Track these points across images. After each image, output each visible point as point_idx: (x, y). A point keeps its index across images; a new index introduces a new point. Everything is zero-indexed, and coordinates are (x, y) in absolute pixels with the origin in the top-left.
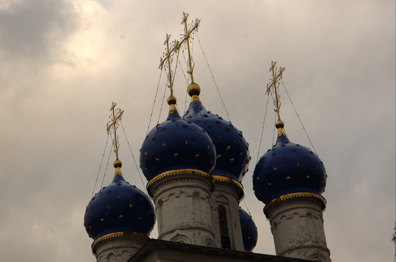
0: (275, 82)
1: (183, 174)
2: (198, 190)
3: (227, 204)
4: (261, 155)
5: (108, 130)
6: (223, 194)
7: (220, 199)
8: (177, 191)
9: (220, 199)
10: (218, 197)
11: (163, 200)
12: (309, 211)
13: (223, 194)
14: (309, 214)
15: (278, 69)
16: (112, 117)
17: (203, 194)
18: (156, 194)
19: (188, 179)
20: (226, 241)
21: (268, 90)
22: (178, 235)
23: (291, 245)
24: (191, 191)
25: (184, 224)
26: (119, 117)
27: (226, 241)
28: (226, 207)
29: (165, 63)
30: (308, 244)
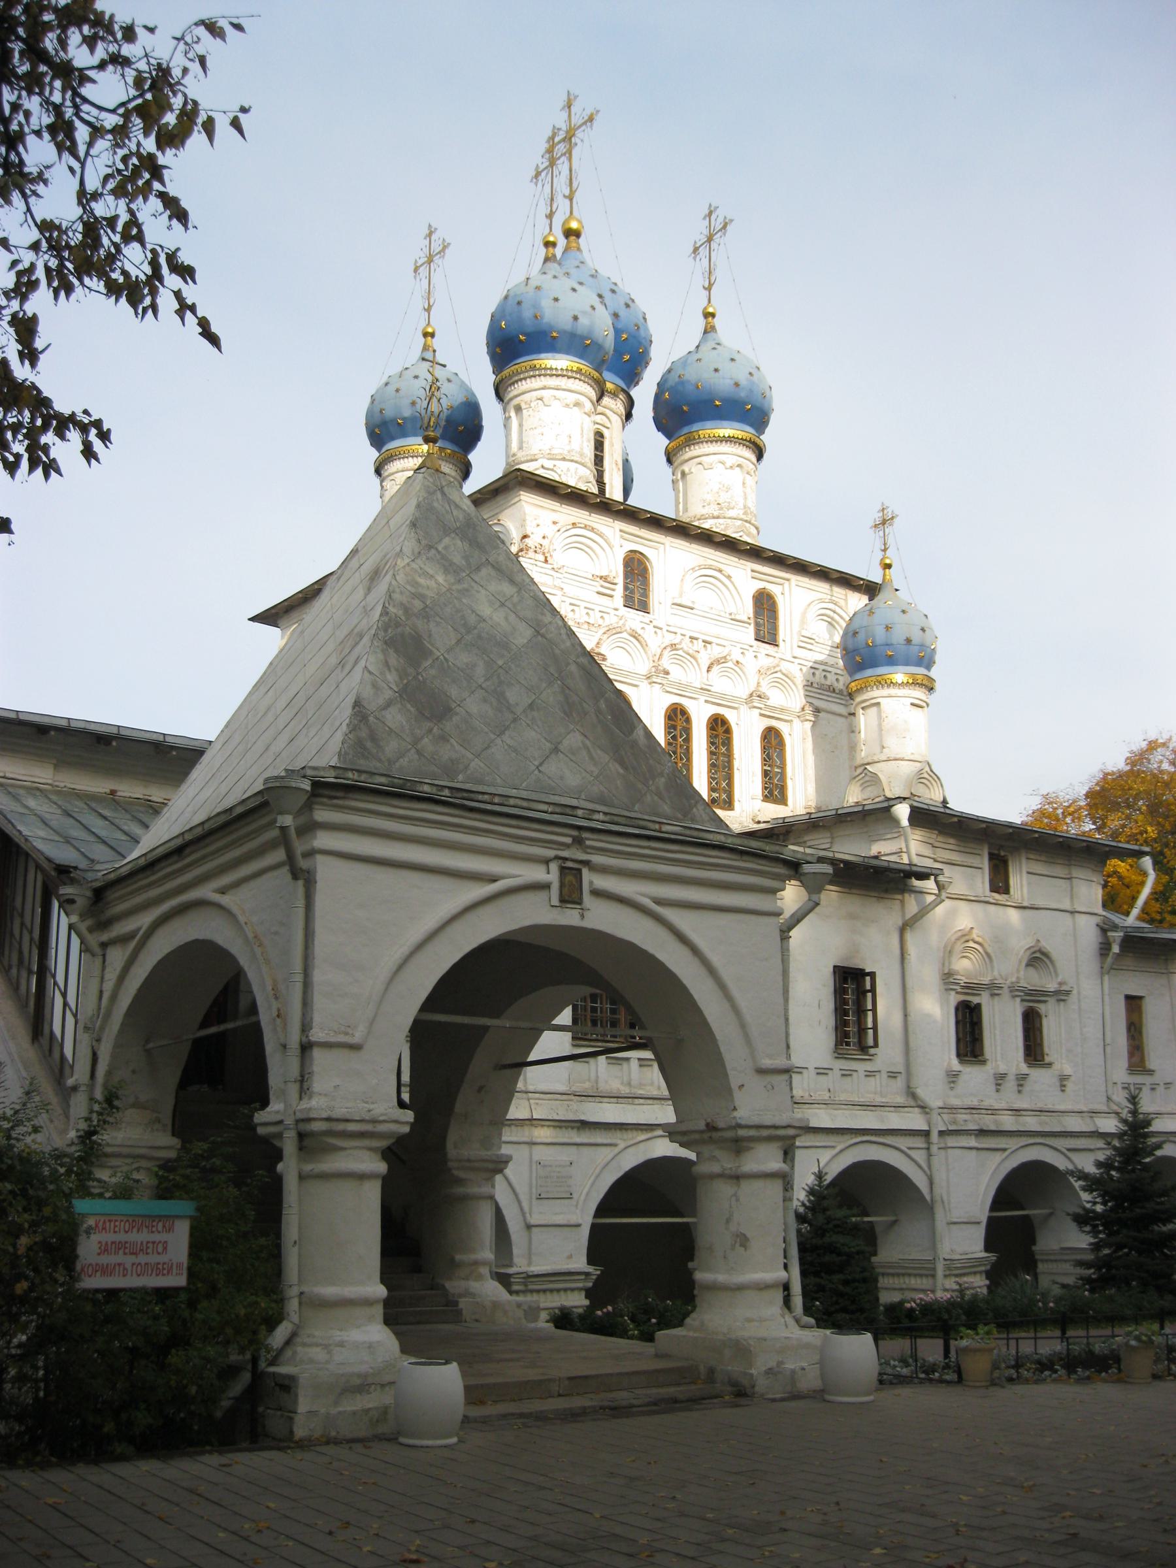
0: (710, 239)
4: (675, 357)
5: (416, 270)
8: (545, 393)
11: (523, 406)
15: (721, 219)
16: (426, 251)
18: (511, 395)
21: (696, 250)
23: (704, 511)
25: (554, 452)
26: (439, 253)
28: (606, 432)
29: (543, 174)
30: (731, 513)
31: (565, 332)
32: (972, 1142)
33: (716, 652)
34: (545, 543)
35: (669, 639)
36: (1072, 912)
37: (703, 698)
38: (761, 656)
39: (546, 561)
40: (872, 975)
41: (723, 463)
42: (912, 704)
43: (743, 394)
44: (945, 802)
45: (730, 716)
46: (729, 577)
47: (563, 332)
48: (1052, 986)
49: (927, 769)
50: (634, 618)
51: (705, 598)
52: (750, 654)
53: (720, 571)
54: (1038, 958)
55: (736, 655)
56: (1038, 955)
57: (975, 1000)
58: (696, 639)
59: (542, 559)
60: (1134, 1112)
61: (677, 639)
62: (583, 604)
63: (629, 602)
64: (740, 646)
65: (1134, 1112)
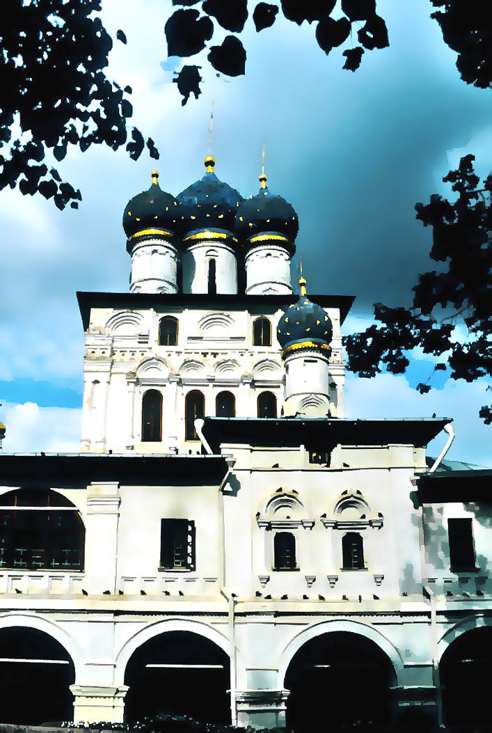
10: (208, 251)
22: (137, 287)
32: (271, 619)
33: (220, 358)
36: (389, 469)
38: (255, 354)
39: (100, 334)
40: (192, 523)
42: (306, 361)
44: (329, 415)
46: (228, 316)
52: (247, 354)
54: (347, 502)
55: (236, 356)
58: (207, 353)
61: (190, 357)
62: (128, 350)
64: (237, 351)
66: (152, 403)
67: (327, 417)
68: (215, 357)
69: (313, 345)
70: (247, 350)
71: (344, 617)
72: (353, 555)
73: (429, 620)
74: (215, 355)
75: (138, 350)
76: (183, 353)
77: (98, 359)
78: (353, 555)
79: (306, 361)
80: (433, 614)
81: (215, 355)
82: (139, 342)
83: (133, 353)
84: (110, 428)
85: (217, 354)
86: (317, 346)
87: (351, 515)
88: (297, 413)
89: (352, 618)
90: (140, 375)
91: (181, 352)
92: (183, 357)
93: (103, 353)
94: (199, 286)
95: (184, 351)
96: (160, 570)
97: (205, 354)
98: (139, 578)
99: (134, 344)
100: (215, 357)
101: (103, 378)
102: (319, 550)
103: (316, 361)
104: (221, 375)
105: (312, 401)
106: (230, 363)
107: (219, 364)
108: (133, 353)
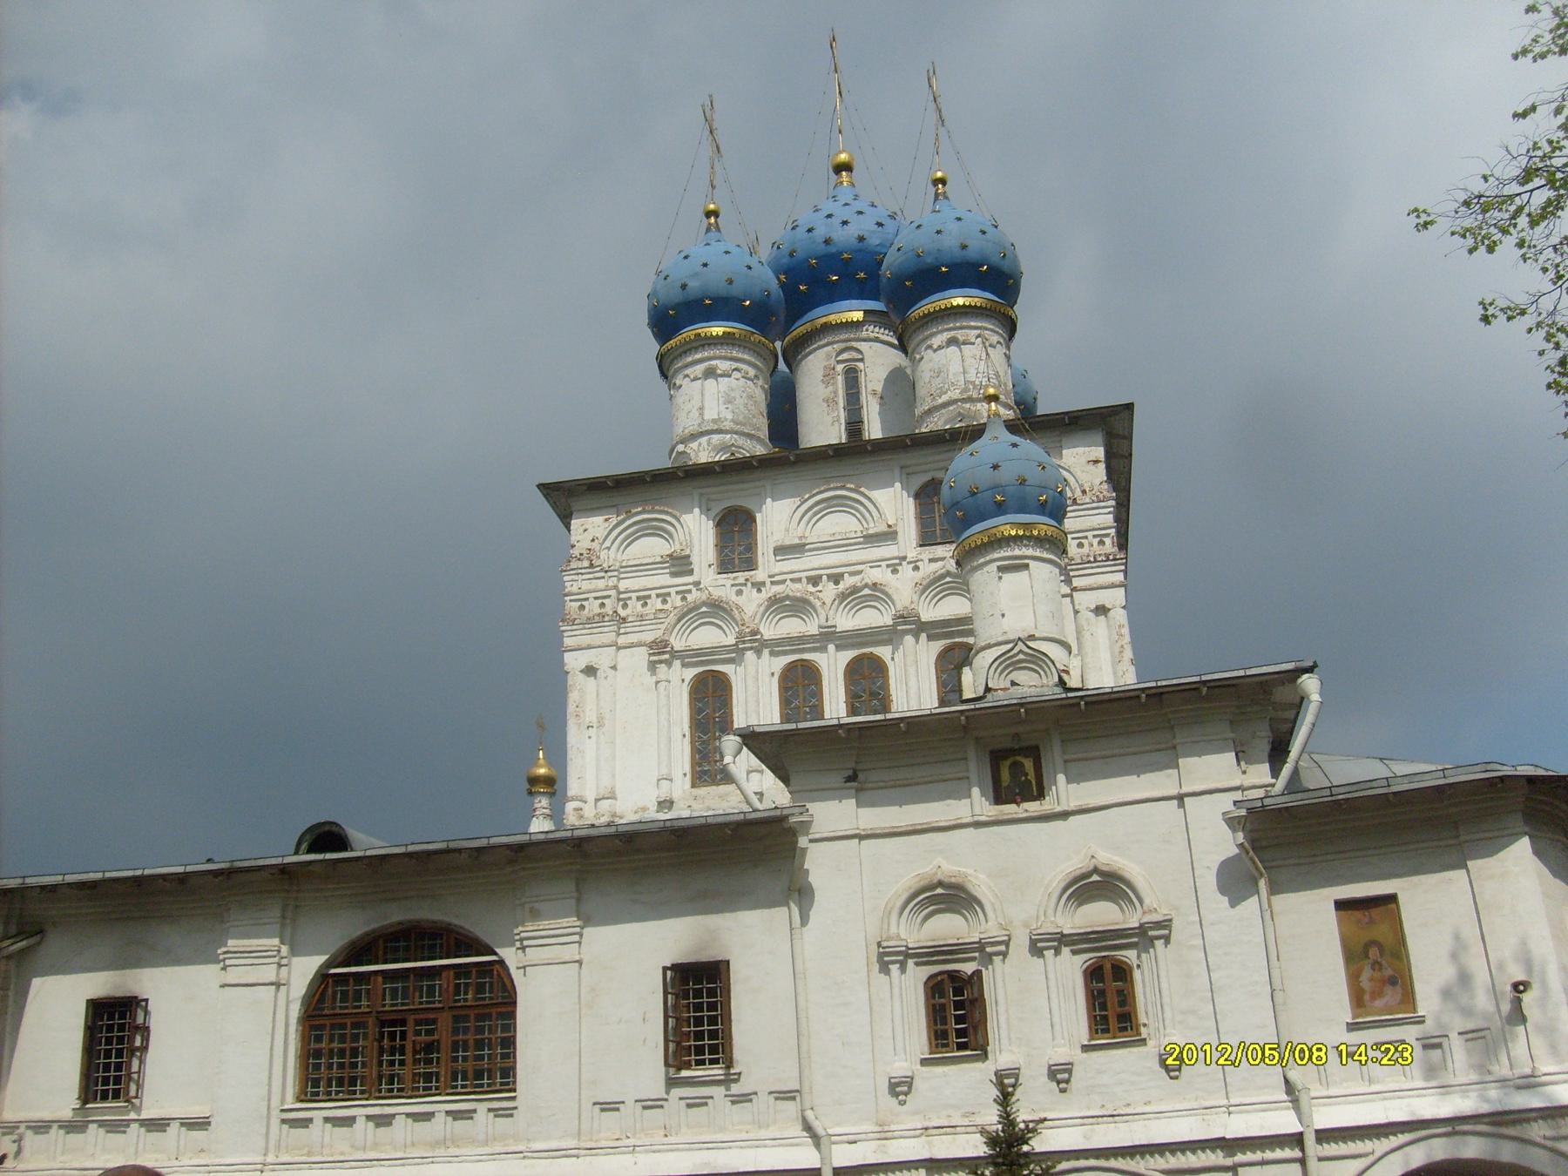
1: (682, 345)
2: (713, 362)
3: (862, 360)
6: (854, 344)
7: (845, 356)
9: (845, 356)
10: (839, 354)
12: (952, 333)
13: (854, 344)
14: (953, 341)
17: (723, 366)
19: (696, 348)
20: (855, 426)
24: (699, 369)
27: (855, 426)
30: (945, 398)
31: (678, 304)
33: (849, 581)
34: (595, 545)
35: (771, 591)
37: (831, 647)
39: (592, 566)
41: (930, 347)
42: (1001, 569)
43: (929, 260)
44: (1062, 682)
45: (883, 652)
47: (676, 307)
48: (1133, 922)
49: (1021, 646)
50: (720, 586)
51: (840, 524)
52: (906, 569)
53: (843, 488)
55: (879, 575)
56: (1095, 878)
57: (968, 968)
58: (820, 577)
59: (586, 563)
60: (1007, 1119)
62: (653, 593)
63: (725, 565)
64: (884, 564)
65: (1007, 1119)
66: (710, 698)
67: (1058, 690)
68: (837, 583)
69: (1013, 533)
70: (904, 558)
71: (1092, 1162)
72: (1112, 1007)
73: (1297, 1153)
74: (836, 579)
75: (673, 591)
76: (768, 584)
77: (590, 620)
78: (1112, 1007)
79: (1000, 569)
80: (1310, 1140)
81: (836, 579)
82: (674, 574)
83: (664, 598)
84: (626, 759)
85: (841, 575)
86: (1021, 533)
87: (1101, 914)
88: (988, 690)
89: (1113, 1163)
90: (678, 644)
91: (763, 584)
92: (765, 595)
93: (603, 605)
94: (821, 425)
95: (768, 581)
96: (671, 1083)
97: (815, 581)
98: (630, 1102)
99: (664, 579)
100: (837, 583)
101: (602, 658)
102: (1036, 1009)
103: (1026, 566)
104: (846, 621)
105: (1021, 656)
106: (867, 591)
107: (843, 597)
108: (664, 598)
